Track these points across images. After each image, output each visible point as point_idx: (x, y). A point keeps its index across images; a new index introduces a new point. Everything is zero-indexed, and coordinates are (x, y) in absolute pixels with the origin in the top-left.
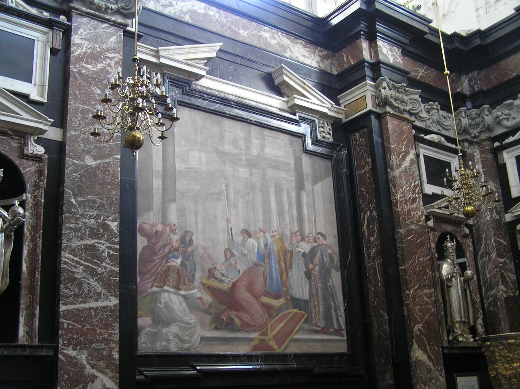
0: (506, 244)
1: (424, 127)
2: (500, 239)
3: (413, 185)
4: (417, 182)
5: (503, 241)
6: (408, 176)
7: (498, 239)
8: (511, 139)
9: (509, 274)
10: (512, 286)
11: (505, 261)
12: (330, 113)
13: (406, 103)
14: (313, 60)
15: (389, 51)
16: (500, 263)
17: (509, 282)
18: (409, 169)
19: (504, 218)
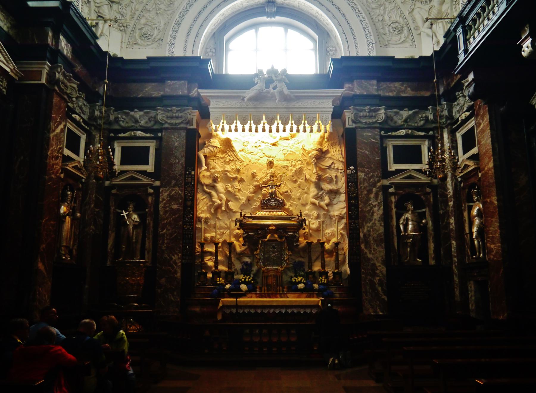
1: (72, 107)
3: (59, 147)
4: (61, 146)
6: (57, 140)
8: (122, 135)
9: (100, 220)
11: (99, 211)
12: (11, 73)
13: (67, 87)
14: (5, 24)
15: (65, 46)
18: (59, 135)
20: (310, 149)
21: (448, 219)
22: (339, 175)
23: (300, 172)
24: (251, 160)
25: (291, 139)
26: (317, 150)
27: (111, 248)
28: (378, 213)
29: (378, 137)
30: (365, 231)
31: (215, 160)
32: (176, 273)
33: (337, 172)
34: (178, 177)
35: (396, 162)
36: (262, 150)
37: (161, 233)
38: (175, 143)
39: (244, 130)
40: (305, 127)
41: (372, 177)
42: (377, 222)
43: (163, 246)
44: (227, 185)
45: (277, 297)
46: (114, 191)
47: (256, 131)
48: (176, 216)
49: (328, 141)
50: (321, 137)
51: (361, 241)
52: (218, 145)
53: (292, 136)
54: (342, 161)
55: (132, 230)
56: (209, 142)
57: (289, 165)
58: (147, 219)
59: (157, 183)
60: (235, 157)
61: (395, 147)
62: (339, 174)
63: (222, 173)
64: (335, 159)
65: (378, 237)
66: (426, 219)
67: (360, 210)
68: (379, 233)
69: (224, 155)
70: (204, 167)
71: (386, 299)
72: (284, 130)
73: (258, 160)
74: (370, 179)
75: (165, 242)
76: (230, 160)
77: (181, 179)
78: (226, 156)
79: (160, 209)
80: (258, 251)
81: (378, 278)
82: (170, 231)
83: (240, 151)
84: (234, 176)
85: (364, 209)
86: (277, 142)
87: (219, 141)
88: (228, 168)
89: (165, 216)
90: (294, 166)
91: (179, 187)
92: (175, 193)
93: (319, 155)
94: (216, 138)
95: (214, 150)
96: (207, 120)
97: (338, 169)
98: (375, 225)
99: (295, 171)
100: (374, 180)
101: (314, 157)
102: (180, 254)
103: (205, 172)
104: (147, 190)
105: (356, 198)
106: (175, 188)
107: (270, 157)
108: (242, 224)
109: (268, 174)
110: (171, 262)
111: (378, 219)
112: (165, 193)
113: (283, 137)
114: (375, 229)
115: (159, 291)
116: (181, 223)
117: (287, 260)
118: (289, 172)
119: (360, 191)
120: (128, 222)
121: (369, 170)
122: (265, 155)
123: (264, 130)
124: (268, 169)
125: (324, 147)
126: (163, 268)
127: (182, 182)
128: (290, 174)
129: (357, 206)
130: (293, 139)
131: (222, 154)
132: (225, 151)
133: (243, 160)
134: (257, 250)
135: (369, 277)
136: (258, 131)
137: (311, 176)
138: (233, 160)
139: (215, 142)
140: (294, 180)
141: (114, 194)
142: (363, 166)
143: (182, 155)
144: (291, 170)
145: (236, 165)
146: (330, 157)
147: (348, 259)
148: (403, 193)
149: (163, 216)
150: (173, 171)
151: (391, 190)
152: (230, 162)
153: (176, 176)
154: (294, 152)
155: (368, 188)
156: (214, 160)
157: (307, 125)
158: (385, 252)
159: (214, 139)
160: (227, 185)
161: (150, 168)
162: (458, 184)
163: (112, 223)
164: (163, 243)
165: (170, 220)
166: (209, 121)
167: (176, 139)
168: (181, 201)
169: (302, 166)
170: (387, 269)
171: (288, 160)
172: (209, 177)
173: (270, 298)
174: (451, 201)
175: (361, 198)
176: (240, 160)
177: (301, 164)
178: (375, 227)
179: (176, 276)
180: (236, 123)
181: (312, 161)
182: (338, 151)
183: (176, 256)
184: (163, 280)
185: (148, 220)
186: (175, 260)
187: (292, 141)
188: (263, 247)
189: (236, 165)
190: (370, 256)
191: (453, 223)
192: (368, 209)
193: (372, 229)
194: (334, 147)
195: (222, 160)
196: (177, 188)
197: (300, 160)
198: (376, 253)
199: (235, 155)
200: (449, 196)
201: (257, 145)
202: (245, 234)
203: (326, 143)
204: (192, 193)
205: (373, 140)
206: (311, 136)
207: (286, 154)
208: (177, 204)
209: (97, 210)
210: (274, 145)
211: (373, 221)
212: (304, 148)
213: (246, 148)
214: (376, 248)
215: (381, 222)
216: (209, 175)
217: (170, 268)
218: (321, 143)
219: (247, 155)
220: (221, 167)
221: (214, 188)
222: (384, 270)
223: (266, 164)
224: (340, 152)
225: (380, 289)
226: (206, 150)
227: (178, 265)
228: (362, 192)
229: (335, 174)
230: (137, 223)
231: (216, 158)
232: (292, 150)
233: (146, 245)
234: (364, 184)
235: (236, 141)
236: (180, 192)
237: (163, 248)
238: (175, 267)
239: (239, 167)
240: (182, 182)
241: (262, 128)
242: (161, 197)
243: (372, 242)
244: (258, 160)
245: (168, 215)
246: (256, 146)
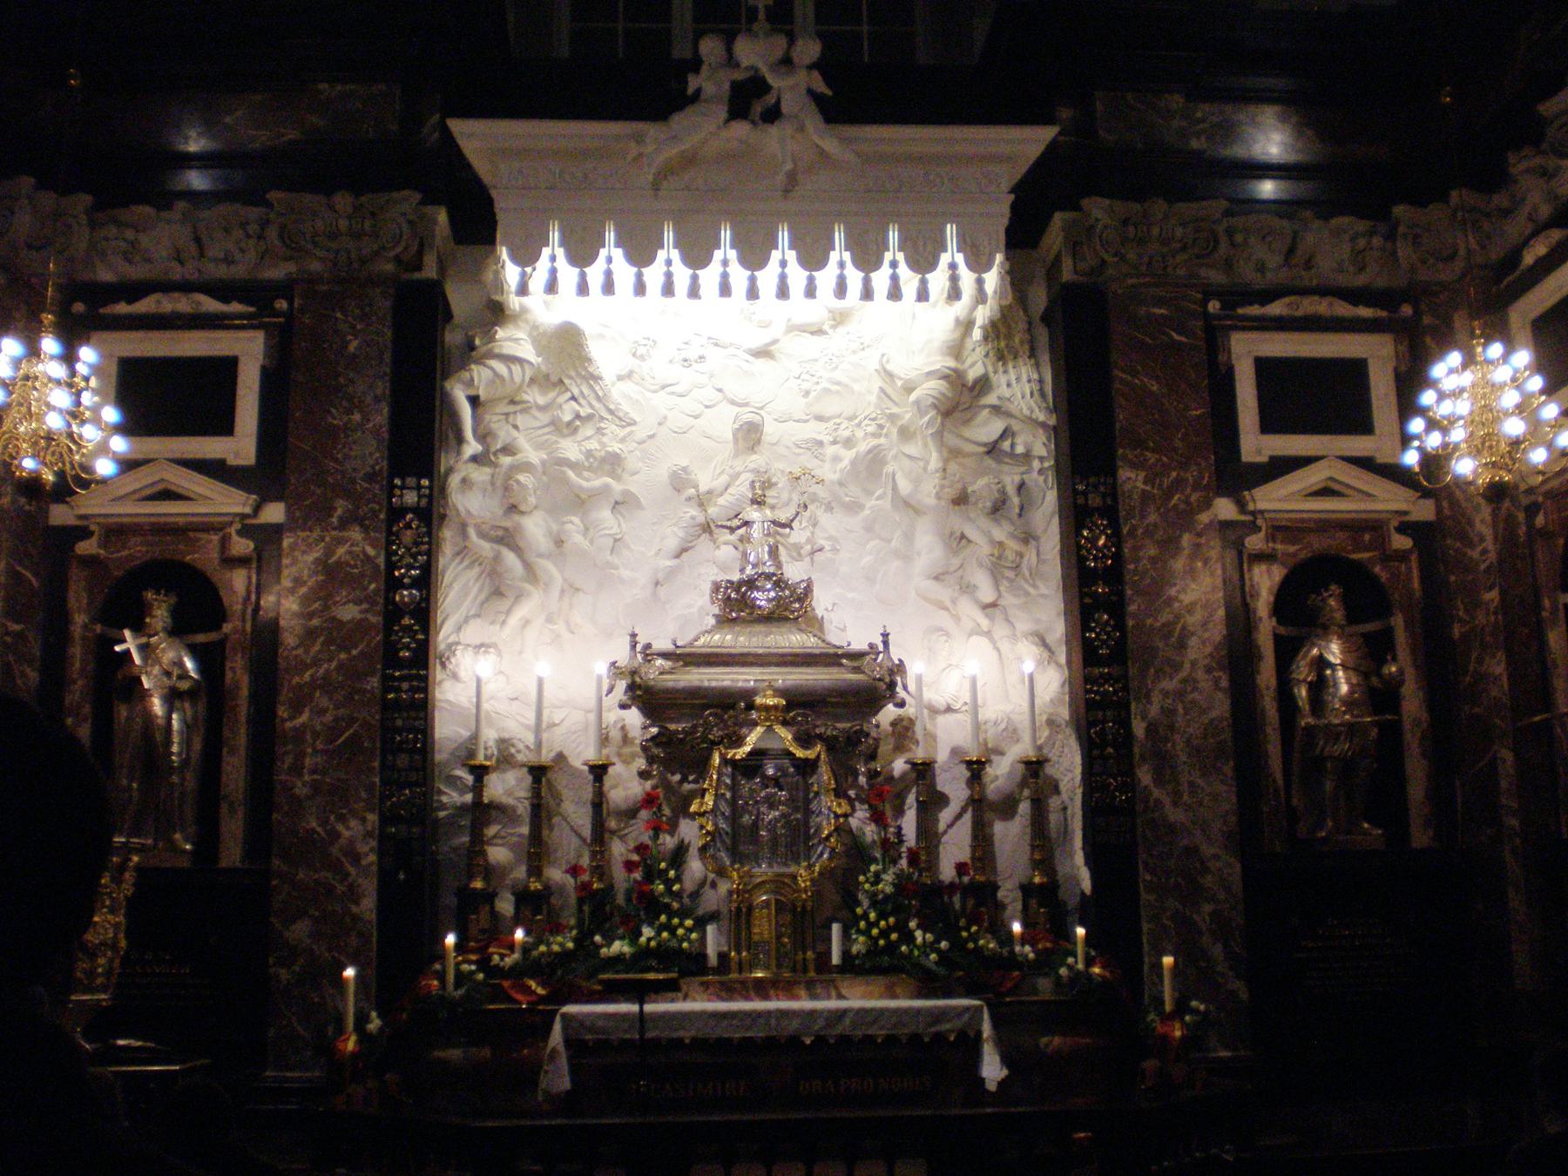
2: (26, 568)
5: (28, 575)
7: (19, 568)
8: (122, 308)
16: (7, 634)
20: (913, 374)
21: (1480, 661)
22: (1034, 479)
23: (871, 466)
24: (665, 418)
25: (830, 331)
26: (945, 377)
28: (1206, 635)
29: (1199, 324)
30: (1154, 710)
31: (511, 419)
32: (354, 895)
33: (1023, 469)
34: (358, 487)
35: (1269, 425)
36: (712, 376)
37: (289, 725)
38: (345, 345)
39: (640, 289)
40: (895, 279)
41: (1179, 484)
42: (1200, 674)
43: (299, 784)
44: (565, 519)
45: (795, 998)
46: (86, 547)
47: (694, 292)
48: (354, 652)
49: (986, 338)
50: (958, 321)
51: (1136, 750)
52: (526, 351)
53: (838, 317)
54: (1043, 425)
56: (492, 339)
57: (827, 439)
58: (228, 664)
59: (274, 513)
60: (595, 403)
61: (1264, 367)
62: (1035, 475)
63: (544, 473)
64: (1017, 414)
65: (1205, 737)
66: (1394, 659)
67: (1131, 623)
68: (1212, 720)
69: (552, 395)
70: (472, 447)
71: (1244, 996)
72: (810, 292)
73: (696, 417)
74: (1168, 495)
75: (307, 761)
76: (578, 416)
77: (375, 495)
78: (561, 399)
80: (709, 800)
81: (1207, 908)
82: (329, 717)
83: (620, 378)
84: (597, 483)
85: (1149, 621)
86: (775, 342)
87: (530, 335)
88: (571, 449)
89: (307, 652)
90: (848, 443)
91: (366, 529)
92: (350, 552)
93: (950, 395)
94: (520, 323)
95: (509, 369)
96: (480, 250)
97: (1027, 456)
98: (1195, 689)
99: (853, 463)
100: (1188, 503)
101: (935, 406)
102: (372, 818)
103: (472, 466)
105: (1114, 575)
106: (345, 534)
107: (746, 405)
108: (640, 687)
109: (738, 475)
110: (335, 851)
111: (1206, 661)
112: (304, 552)
113: (799, 320)
114: (1193, 702)
115: (284, 974)
116: (374, 682)
117: (830, 835)
118: (827, 466)
119: (1128, 545)
120: (144, 679)
121: (1165, 459)
122: (725, 398)
123: (725, 290)
124: (736, 455)
125: (969, 361)
126: (301, 875)
127: (377, 507)
128: (829, 473)
129: (1117, 608)
130: (840, 330)
131: (544, 393)
132: (554, 379)
133: (634, 415)
134: (703, 792)
135: (1172, 904)
136: (701, 292)
137: (917, 482)
138: (590, 417)
139: (514, 341)
140: (848, 499)
141: (90, 561)
142: (1140, 444)
143: (379, 392)
144: (836, 459)
145: (605, 439)
146: (996, 410)
147: (1084, 829)
148: (1302, 555)
150: (336, 460)
151: (1255, 542)
152: (578, 423)
153: (353, 481)
154: (847, 386)
155: (1159, 535)
156: (507, 414)
157: (904, 271)
158: (1234, 800)
159: (511, 326)
160: (565, 519)
161: (241, 446)
162: (1521, 516)
164: (297, 770)
165: (327, 671)
166: (493, 251)
167: (354, 327)
168: (373, 586)
169: (882, 440)
170: (1244, 867)
171: (820, 418)
172: (490, 488)
173: (766, 997)
174: (1491, 589)
175: (1135, 572)
176: (621, 414)
177: (874, 435)
178: (1195, 695)
179: (354, 909)
180: (609, 260)
181: (926, 419)
182: (1029, 381)
183: (353, 823)
184: (300, 931)
186: (351, 841)
187: (838, 340)
188: (728, 781)
189: (605, 439)
190: (1175, 815)
191: (1501, 674)
192: (1163, 620)
193: (1182, 702)
194: (1010, 365)
195: (544, 418)
196: (356, 534)
197: (874, 415)
198: (1201, 804)
199: (600, 393)
200: (1483, 567)
201: (692, 354)
202: (652, 725)
203: (978, 350)
204: (420, 553)
205: (1176, 337)
206: (914, 317)
207: (813, 394)
208: (358, 602)
209: (17, 627)
210: (763, 353)
211: (1187, 665)
212: (889, 367)
213: (643, 364)
214: (1199, 781)
215: (1216, 674)
216: (488, 478)
217: (329, 875)
218: (956, 349)
219: (648, 394)
220: (539, 446)
221: (508, 538)
222: (1234, 870)
223: (730, 436)
224: (1036, 387)
225: (1217, 951)
226: (481, 376)
227: (364, 862)
228: (1136, 549)
229: (1017, 479)
230: (184, 686)
231: (519, 407)
232: (838, 375)
234: (1143, 517)
235: (601, 336)
236: (371, 552)
237: (297, 791)
238: (352, 870)
239: (615, 447)
240: (377, 507)
241: (717, 280)
242: (285, 572)
243: (1183, 758)
244: (696, 417)
245: (317, 647)
246: (686, 361)
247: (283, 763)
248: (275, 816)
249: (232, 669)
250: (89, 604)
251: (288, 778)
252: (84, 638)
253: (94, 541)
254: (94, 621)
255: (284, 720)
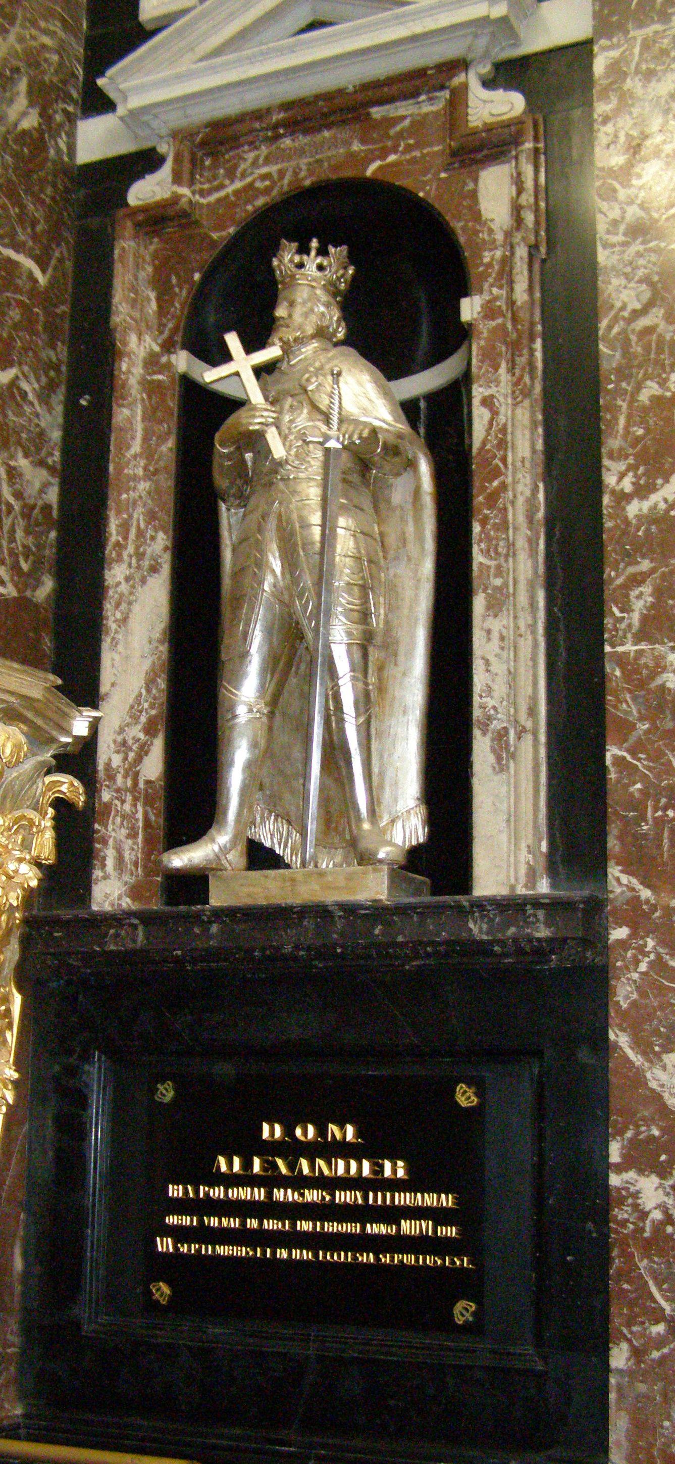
0: (42, 279)
5: (28, 263)
9: (22, 463)
10: (19, 534)
11: (14, 383)
17: (10, 508)
19: (72, 135)
27: (136, 732)
37: (633, 509)
55: (316, 518)
58: (478, 392)
79: (603, 256)
104: (459, 99)
112: (649, 75)
149: (643, 322)
163: (144, 486)
185: (488, 402)
233: (479, 679)
247: (626, 608)
248: (612, 752)
249: (488, 402)
250: (162, 311)
251: (643, 646)
252: (152, 389)
253: (166, 171)
254: (168, 347)
255: (623, 498)
